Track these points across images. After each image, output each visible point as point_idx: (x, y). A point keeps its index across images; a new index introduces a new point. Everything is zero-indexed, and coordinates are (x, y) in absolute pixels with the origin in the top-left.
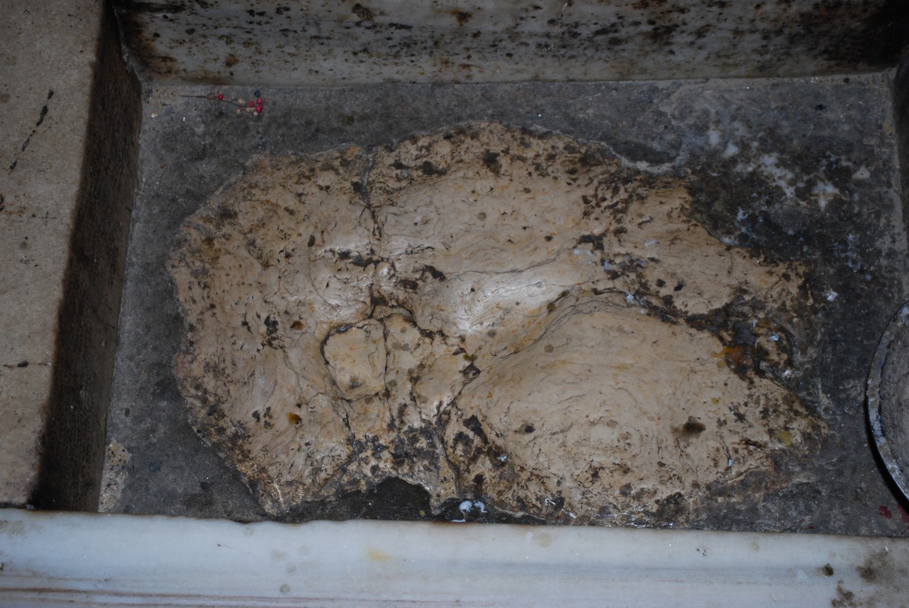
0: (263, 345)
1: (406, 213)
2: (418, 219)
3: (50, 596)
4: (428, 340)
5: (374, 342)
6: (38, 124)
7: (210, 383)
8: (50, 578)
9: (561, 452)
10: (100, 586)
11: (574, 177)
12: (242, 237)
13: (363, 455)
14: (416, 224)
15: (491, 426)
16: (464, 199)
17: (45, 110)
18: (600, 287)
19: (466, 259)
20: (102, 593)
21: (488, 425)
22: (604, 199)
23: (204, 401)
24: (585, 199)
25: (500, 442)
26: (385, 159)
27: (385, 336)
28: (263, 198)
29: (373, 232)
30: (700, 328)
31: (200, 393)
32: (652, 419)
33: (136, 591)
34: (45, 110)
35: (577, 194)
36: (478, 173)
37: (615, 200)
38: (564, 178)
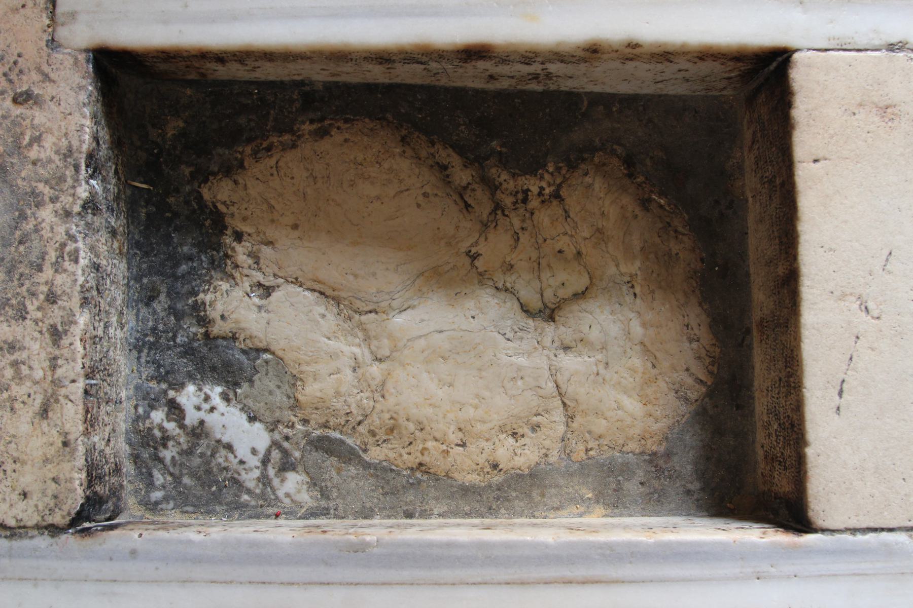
1: (530, 389)
6: (843, 381)
13: (552, 188)
14: (522, 378)
16: (483, 401)
17: (840, 393)
18: (373, 315)
19: (479, 344)
21: (458, 204)
23: (676, 231)
32: (333, 200)
34: (840, 393)
35: (391, 401)
36: (472, 426)
37: (359, 397)
38: (402, 421)
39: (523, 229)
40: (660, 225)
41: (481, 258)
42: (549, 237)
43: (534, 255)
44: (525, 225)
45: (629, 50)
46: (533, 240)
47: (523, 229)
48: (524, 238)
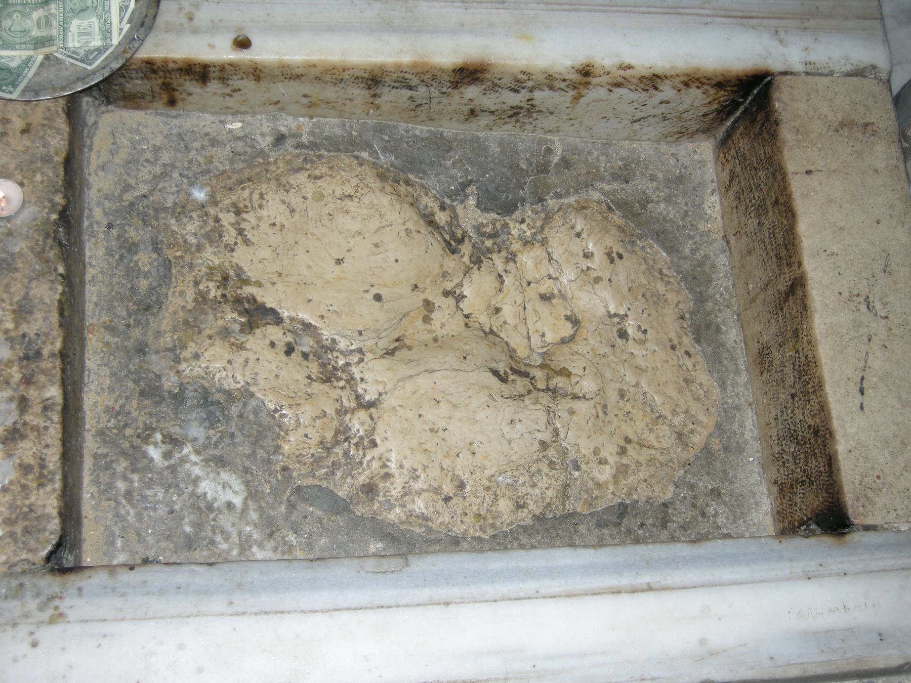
0: (626, 315)
2: (519, 426)
3: (740, 14)
4: (495, 329)
5: (537, 331)
6: (863, 378)
7: (661, 287)
8: (743, 25)
9: (383, 211)
10: (709, 20)
11: (386, 470)
12: (664, 413)
15: (440, 243)
16: (481, 445)
17: (862, 392)
20: (707, 16)
22: (357, 445)
24: (374, 444)
25: (430, 229)
26: (555, 496)
27: (529, 338)
28: (653, 451)
29: (555, 415)
30: (273, 311)
31: (666, 278)
32: (312, 234)
33: (686, 17)
34: (862, 392)
39: (506, 271)
40: (644, 267)
41: (466, 300)
42: (533, 280)
43: (519, 300)
44: (508, 268)
45: (622, 72)
46: (517, 283)
47: (506, 271)
48: (508, 280)
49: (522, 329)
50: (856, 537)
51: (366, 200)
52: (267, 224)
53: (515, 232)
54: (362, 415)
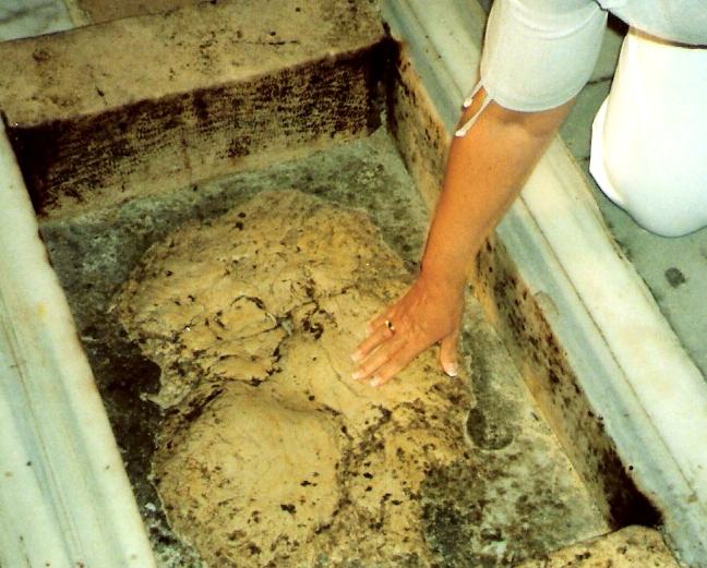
6: (271, 44)
9: (206, 443)
17: (282, 43)
18: (350, 431)
23: (172, 246)
27: (268, 331)
49: (262, 337)
50: (396, 34)
51: (201, 459)
52: (259, 525)
53: (174, 358)
54: (396, 416)
